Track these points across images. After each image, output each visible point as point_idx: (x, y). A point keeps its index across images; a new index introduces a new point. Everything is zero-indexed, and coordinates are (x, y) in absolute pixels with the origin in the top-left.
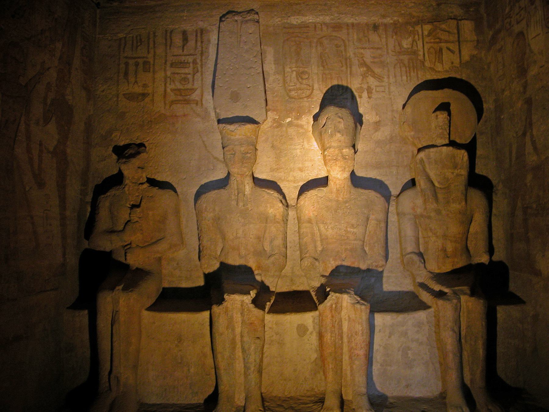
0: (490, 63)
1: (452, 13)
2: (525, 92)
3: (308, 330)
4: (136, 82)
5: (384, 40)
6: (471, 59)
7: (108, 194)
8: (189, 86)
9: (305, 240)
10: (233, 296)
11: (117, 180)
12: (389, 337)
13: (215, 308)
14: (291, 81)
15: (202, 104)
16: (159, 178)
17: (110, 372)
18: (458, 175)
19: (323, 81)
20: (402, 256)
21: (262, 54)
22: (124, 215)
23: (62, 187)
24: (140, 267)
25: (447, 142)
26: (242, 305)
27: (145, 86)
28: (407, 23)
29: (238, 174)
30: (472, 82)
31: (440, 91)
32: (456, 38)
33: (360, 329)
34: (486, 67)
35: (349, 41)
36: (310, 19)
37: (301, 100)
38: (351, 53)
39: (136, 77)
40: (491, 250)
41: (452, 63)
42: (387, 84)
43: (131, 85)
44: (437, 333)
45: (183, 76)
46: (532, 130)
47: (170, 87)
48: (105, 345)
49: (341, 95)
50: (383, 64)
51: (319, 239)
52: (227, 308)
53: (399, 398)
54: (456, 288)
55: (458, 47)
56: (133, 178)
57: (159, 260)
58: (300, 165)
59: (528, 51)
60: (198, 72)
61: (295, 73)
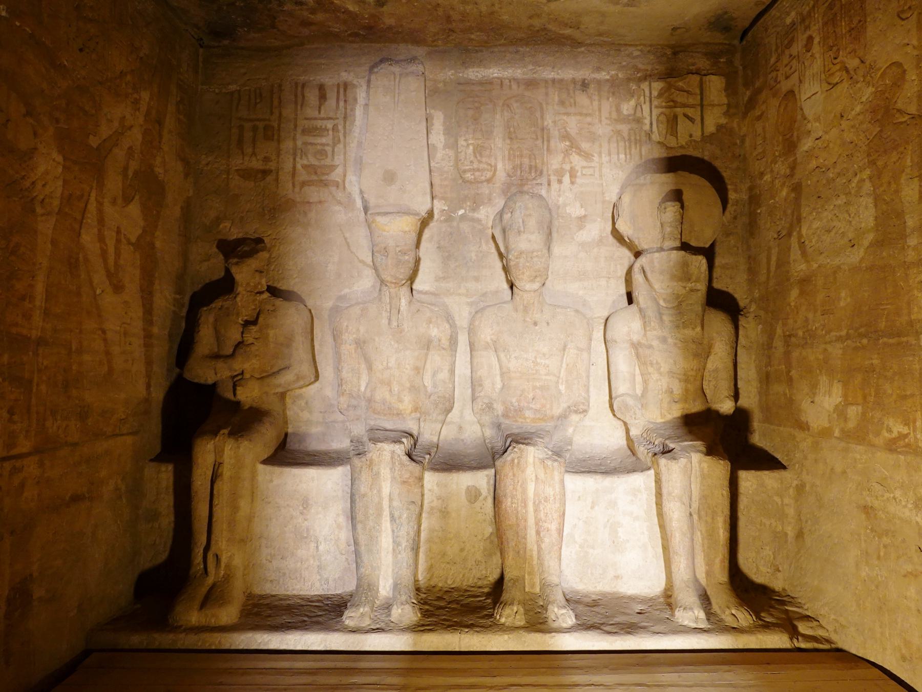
0: (745, 136)
1: (693, 64)
2: (792, 175)
3: (480, 494)
4: (254, 154)
5: (596, 103)
6: (717, 130)
7: (213, 305)
8: (328, 162)
9: (479, 373)
10: (380, 445)
11: (225, 286)
12: (592, 508)
13: (356, 461)
14: (466, 158)
15: (344, 187)
16: (282, 285)
17: (207, 548)
18: (692, 290)
19: (509, 159)
22: (234, 334)
24: (255, 405)
25: (678, 244)
26: (392, 458)
27: (266, 159)
28: (629, 80)
29: (391, 283)
30: (717, 164)
31: (671, 175)
32: (699, 102)
33: (552, 493)
34: (738, 142)
35: (547, 104)
36: (494, 72)
37: (480, 185)
38: (549, 121)
39: (254, 148)
40: (736, 396)
41: (691, 136)
42: (597, 165)
43: (247, 158)
44: (659, 504)
45: (319, 147)
46: (800, 227)
48: (201, 510)
49: (534, 179)
50: (593, 138)
51: (498, 372)
52: (371, 461)
53: (604, 595)
54: (686, 443)
55: (699, 113)
56: (248, 284)
57: (283, 396)
58: (476, 274)
59: (799, 117)
61: (471, 147)
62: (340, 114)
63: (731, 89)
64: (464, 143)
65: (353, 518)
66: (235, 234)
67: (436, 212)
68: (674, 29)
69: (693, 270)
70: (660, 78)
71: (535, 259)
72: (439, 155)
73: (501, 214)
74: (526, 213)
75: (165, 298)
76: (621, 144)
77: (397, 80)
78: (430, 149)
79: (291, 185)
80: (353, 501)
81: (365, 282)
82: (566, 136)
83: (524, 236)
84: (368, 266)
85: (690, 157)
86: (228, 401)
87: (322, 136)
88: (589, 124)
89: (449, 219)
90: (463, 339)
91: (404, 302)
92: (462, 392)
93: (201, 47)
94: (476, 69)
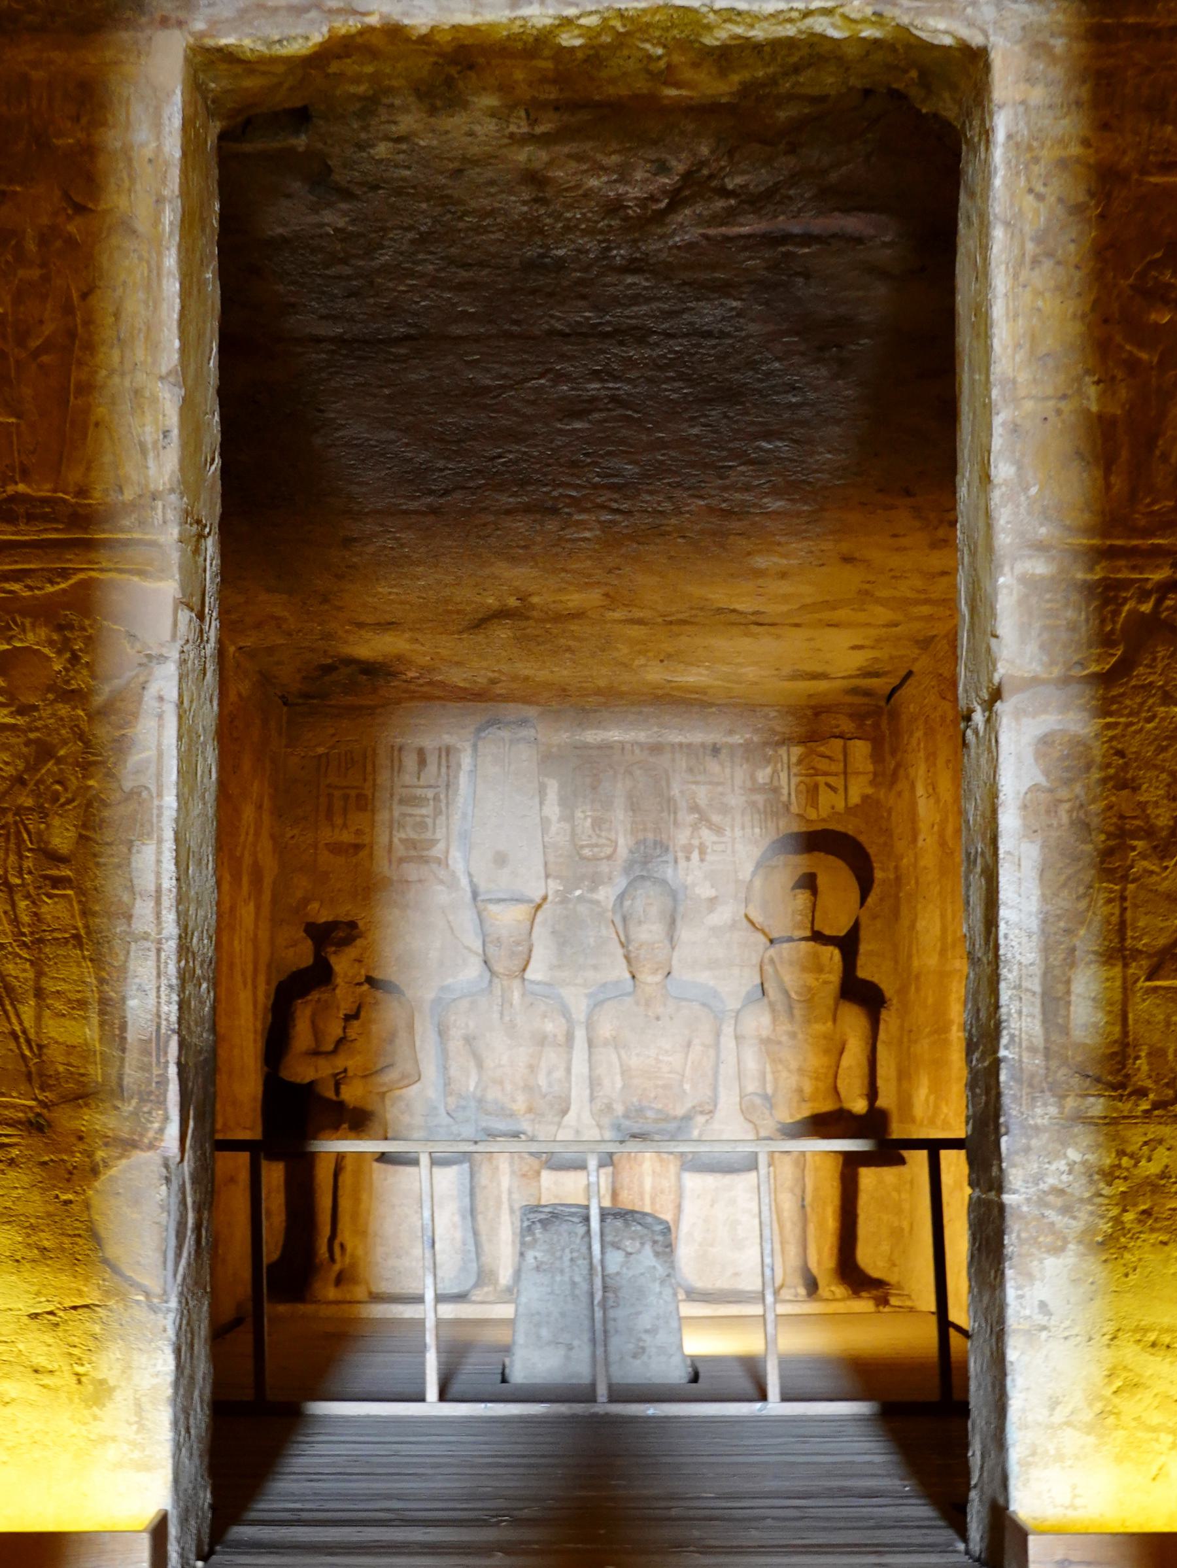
1: (837, 726)
4: (345, 826)
5: (728, 770)
8: (428, 835)
11: (319, 975)
16: (377, 975)
18: (825, 982)
20: (741, 1098)
21: (542, 791)
22: (335, 1030)
23: (255, 987)
25: (808, 934)
28: (766, 744)
30: (862, 839)
36: (615, 735)
38: (675, 791)
40: (872, 1093)
43: (337, 831)
47: (399, 835)
50: (725, 810)
51: (618, 1070)
56: (346, 975)
57: (383, 1095)
60: (441, 812)
63: (877, 756)
65: (472, 1213)
66: (324, 916)
67: (550, 893)
68: (810, 696)
69: (825, 959)
70: (802, 742)
72: (554, 828)
73: (621, 897)
74: (648, 902)
75: (264, 992)
76: (756, 816)
78: (545, 822)
79: (386, 862)
80: (472, 1194)
81: (472, 970)
82: (694, 808)
83: (645, 927)
84: (477, 954)
85: (833, 831)
86: (329, 1101)
89: (564, 901)
90: (580, 1035)
91: (516, 996)
92: (579, 1093)
93: (285, 704)
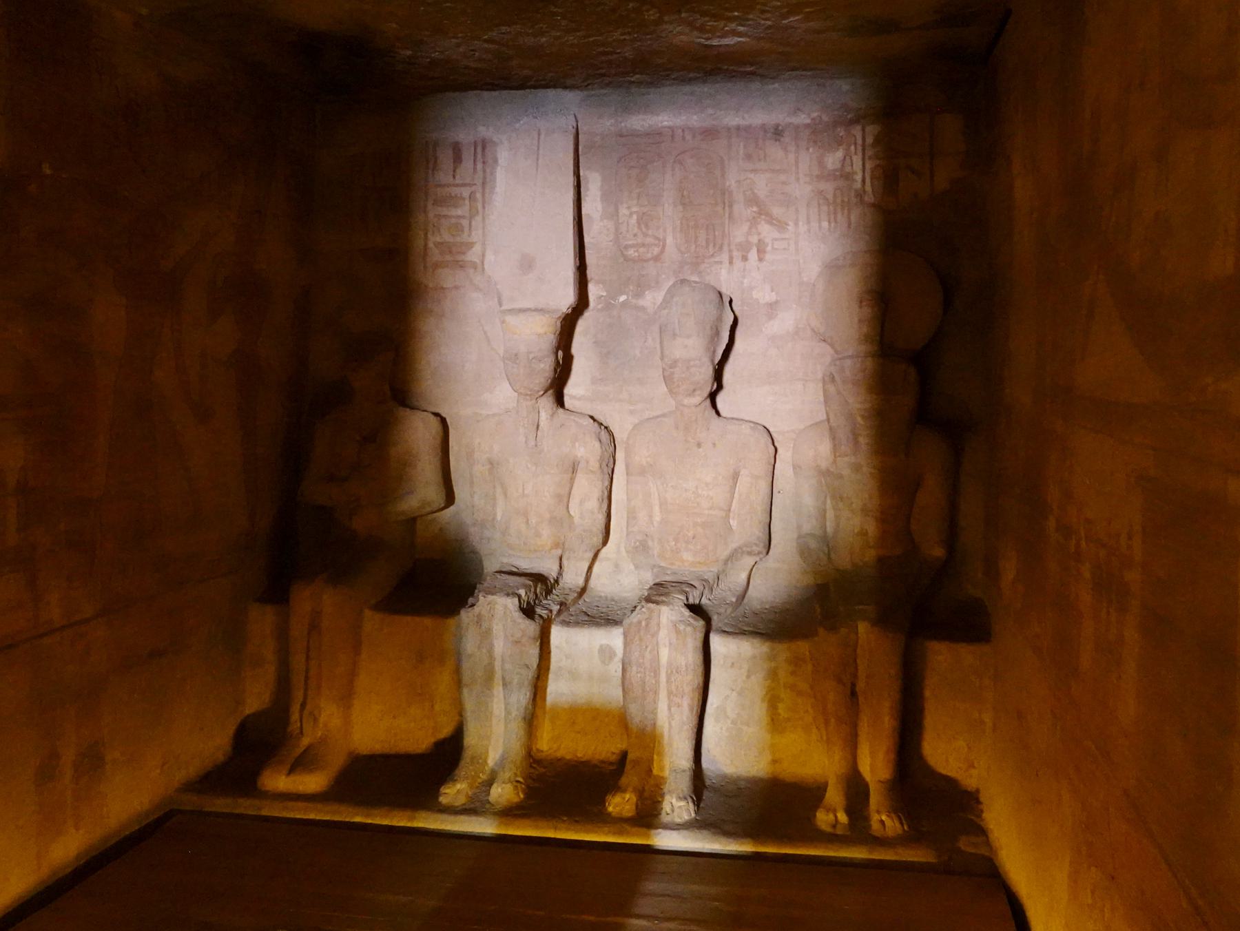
5: (792, 157)
15: (483, 269)
28: (836, 124)
36: (664, 119)
38: (731, 181)
45: (453, 221)
47: (433, 239)
61: (635, 217)
62: (479, 181)
64: (626, 212)
71: (693, 370)
76: (825, 208)
77: (542, 137)
82: (753, 200)
87: (456, 207)
88: (784, 183)
89: (608, 307)
94: (641, 117)
